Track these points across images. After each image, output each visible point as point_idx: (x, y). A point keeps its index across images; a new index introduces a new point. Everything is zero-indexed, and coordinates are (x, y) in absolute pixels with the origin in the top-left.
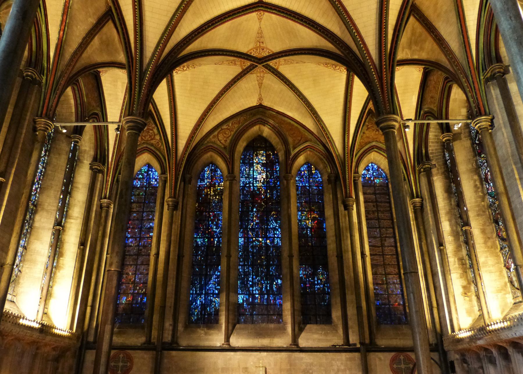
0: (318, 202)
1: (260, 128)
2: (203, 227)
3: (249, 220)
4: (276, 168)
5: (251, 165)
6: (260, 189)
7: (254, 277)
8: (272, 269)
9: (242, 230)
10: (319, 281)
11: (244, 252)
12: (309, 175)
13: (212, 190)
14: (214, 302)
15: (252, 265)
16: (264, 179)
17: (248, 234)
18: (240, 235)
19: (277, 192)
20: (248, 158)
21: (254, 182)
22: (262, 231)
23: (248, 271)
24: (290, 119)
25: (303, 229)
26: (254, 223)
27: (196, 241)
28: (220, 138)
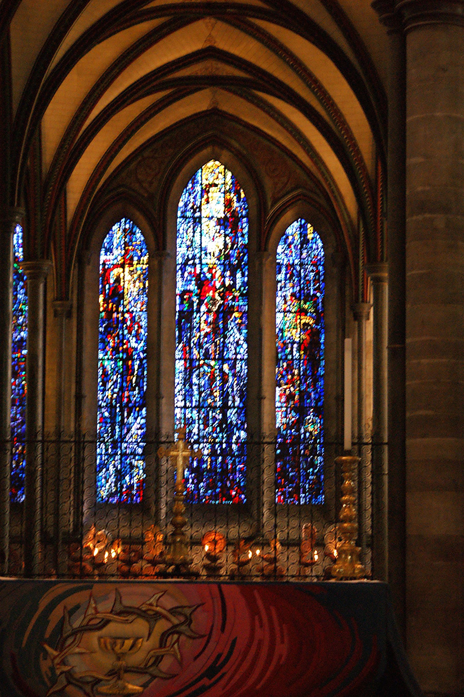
0: (315, 295)
1: (213, 150)
2: (114, 340)
3: (191, 328)
4: (242, 229)
5: (197, 221)
6: (213, 268)
7: (202, 427)
8: (232, 415)
9: (181, 345)
10: (308, 434)
11: (184, 385)
12: (302, 243)
13: (127, 269)
14: (137, 467)
15: (199, 408)
16: (221, 251)
17: (191, 353)
18: (178, 354)
19: (243, 275)
20: (192, 208)
21: (203, 256)
22: (216, 346)
23: (191, 417)
24: (269, 140)
25: (285, 344)
26: (203, 333)
27: (103, 366)
28: (139, 177)
